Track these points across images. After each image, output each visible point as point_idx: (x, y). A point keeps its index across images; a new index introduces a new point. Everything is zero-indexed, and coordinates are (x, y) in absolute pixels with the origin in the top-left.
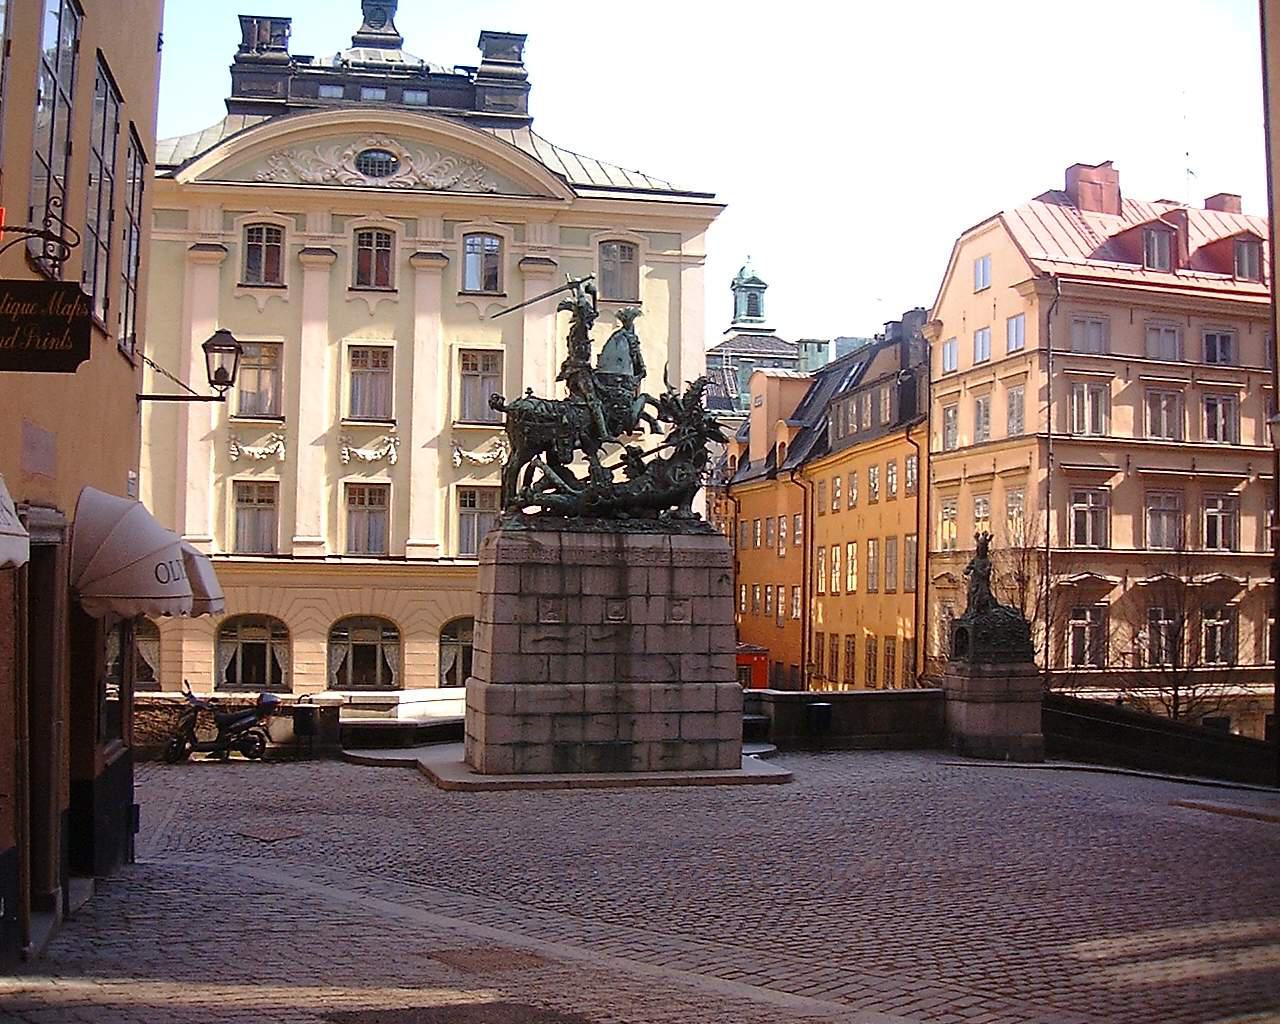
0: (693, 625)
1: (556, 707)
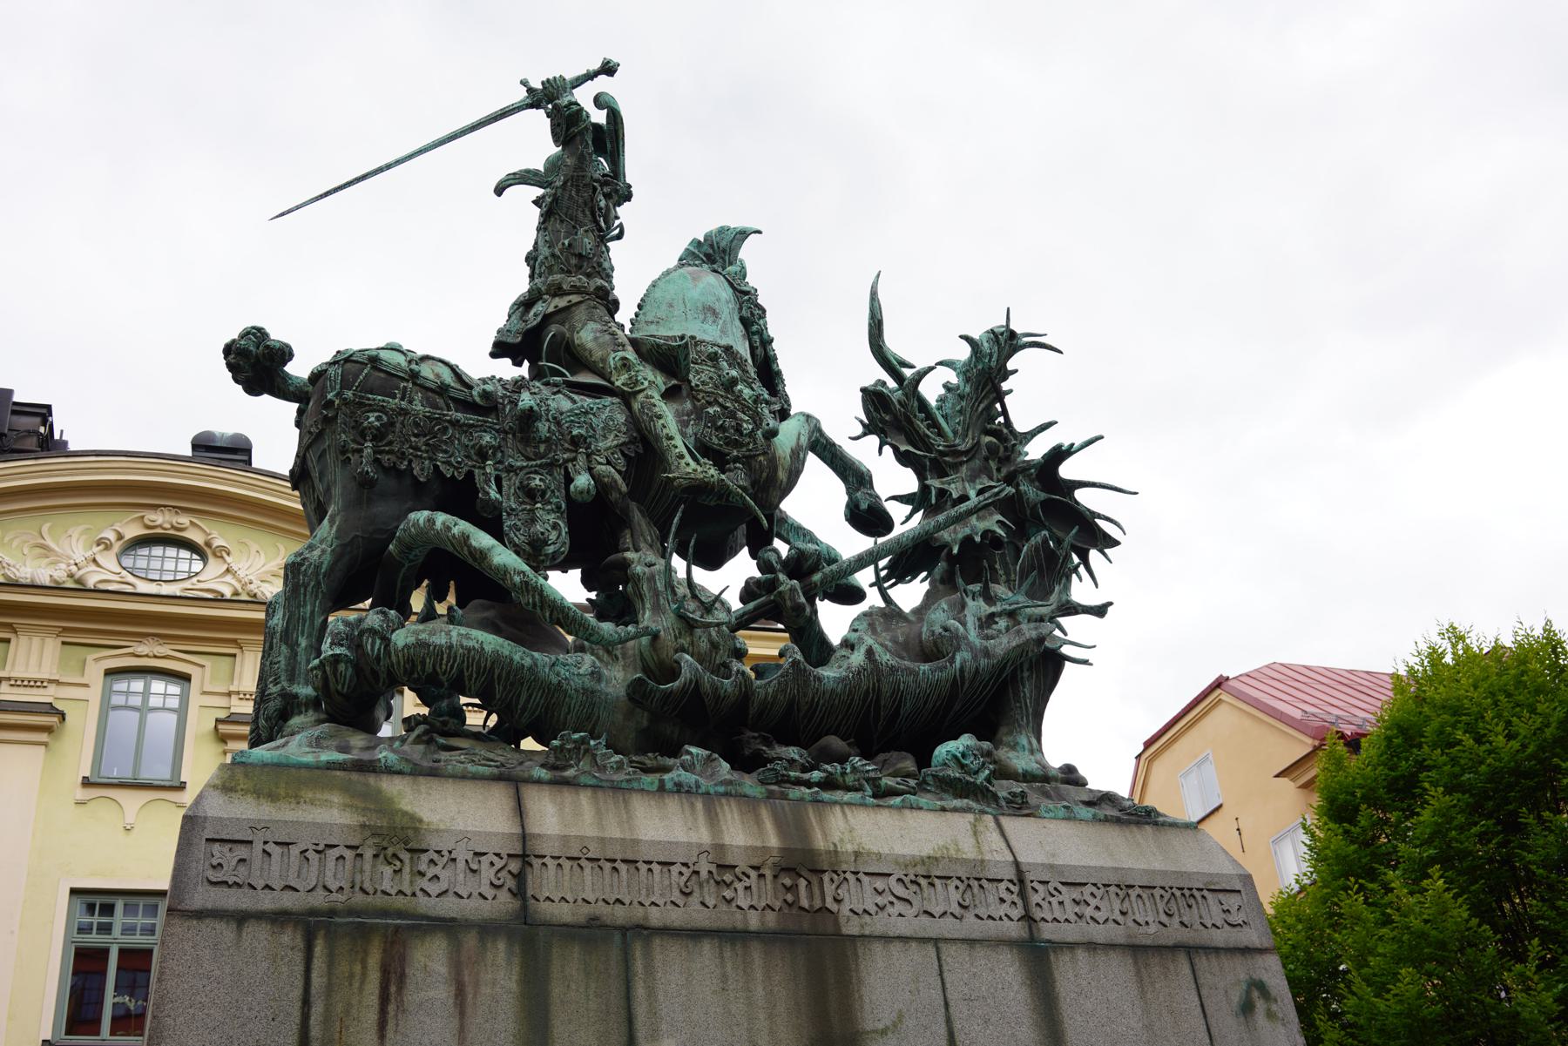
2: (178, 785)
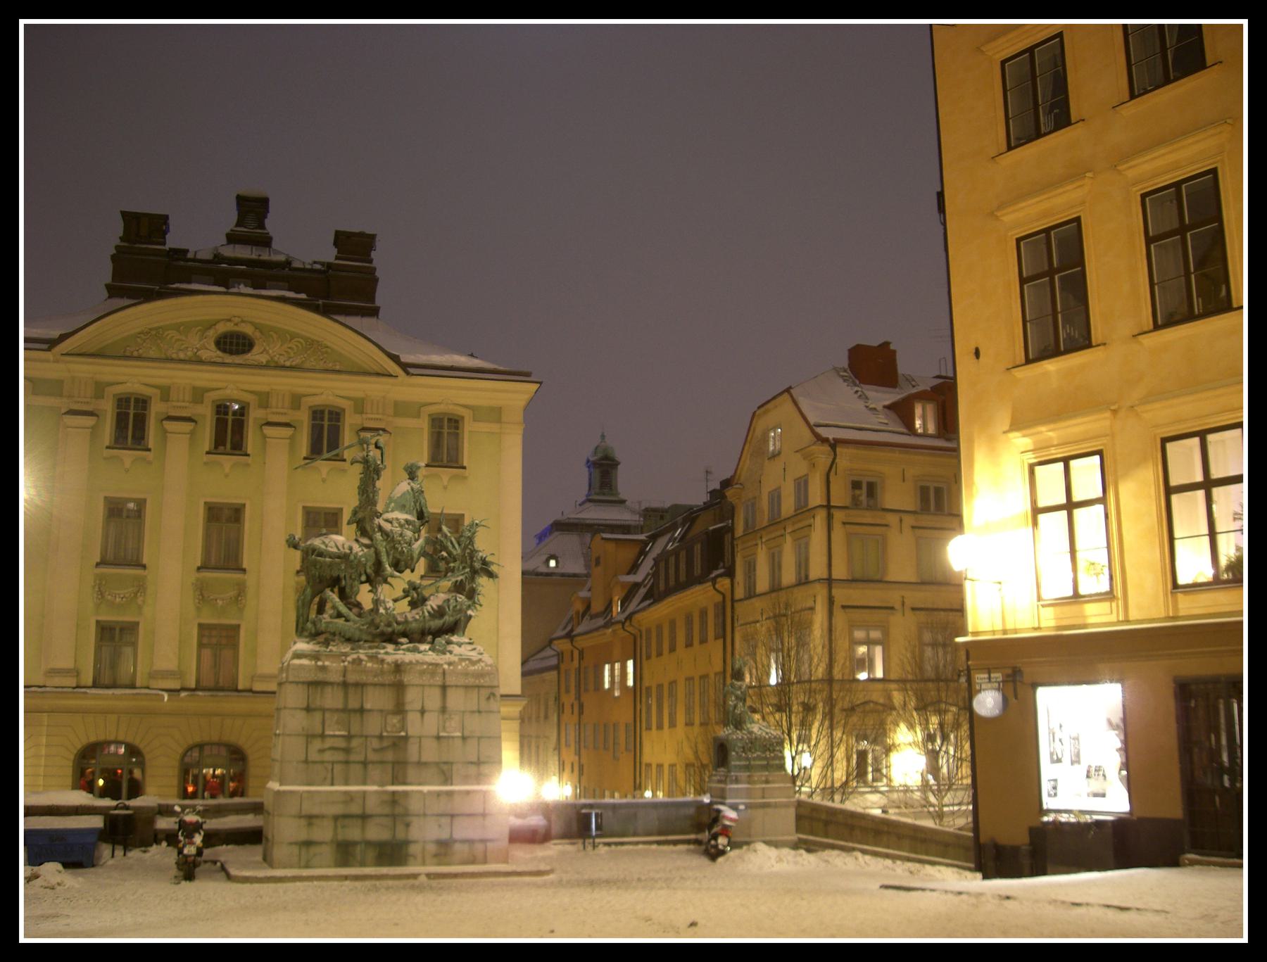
0: (464, 738)
1: (338, 809)
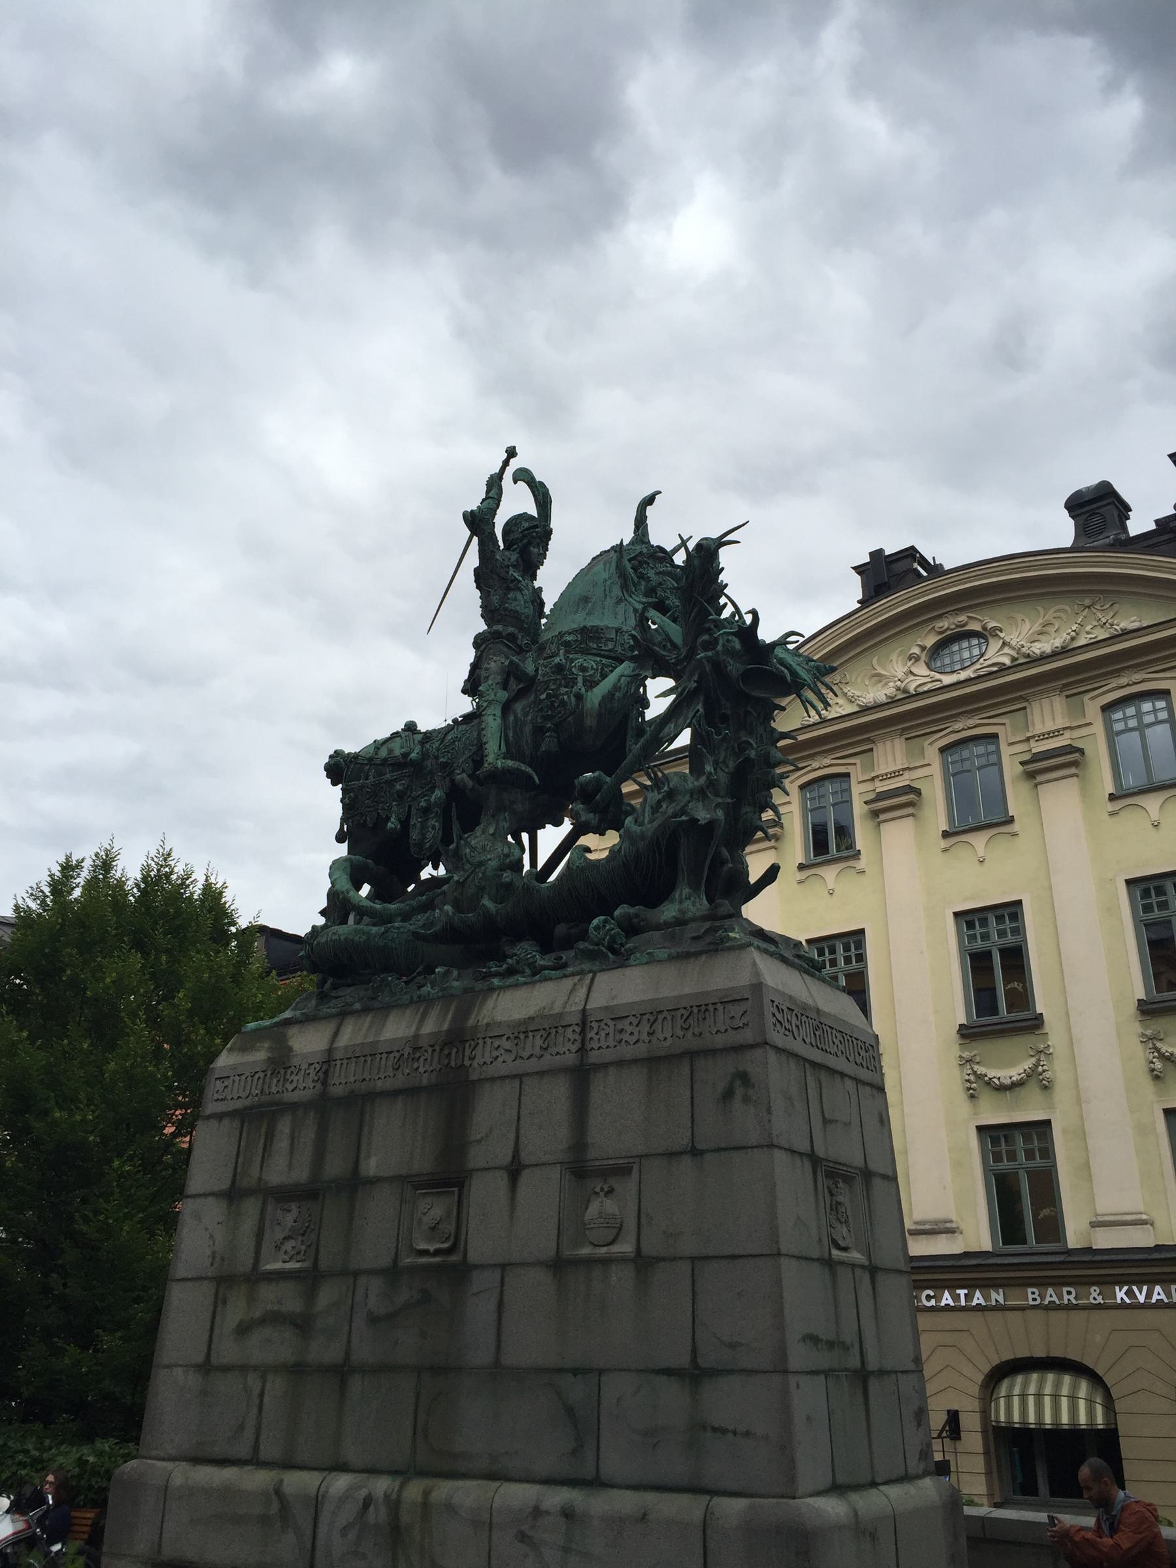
0: (642, 1263)
2: (1008, 819)
